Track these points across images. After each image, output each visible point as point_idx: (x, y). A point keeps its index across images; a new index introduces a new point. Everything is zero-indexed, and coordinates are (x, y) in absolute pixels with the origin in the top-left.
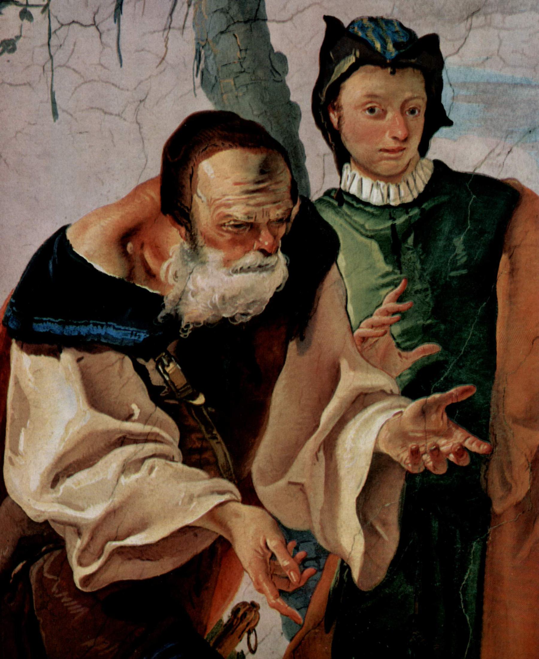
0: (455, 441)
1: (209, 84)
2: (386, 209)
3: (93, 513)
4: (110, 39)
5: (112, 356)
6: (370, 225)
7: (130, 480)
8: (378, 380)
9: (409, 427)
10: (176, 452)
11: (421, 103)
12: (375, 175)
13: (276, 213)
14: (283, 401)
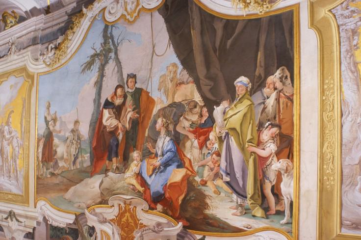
1: (118, 82)
2: (132, 92)
3: (108, 124)
8: (131, 110)
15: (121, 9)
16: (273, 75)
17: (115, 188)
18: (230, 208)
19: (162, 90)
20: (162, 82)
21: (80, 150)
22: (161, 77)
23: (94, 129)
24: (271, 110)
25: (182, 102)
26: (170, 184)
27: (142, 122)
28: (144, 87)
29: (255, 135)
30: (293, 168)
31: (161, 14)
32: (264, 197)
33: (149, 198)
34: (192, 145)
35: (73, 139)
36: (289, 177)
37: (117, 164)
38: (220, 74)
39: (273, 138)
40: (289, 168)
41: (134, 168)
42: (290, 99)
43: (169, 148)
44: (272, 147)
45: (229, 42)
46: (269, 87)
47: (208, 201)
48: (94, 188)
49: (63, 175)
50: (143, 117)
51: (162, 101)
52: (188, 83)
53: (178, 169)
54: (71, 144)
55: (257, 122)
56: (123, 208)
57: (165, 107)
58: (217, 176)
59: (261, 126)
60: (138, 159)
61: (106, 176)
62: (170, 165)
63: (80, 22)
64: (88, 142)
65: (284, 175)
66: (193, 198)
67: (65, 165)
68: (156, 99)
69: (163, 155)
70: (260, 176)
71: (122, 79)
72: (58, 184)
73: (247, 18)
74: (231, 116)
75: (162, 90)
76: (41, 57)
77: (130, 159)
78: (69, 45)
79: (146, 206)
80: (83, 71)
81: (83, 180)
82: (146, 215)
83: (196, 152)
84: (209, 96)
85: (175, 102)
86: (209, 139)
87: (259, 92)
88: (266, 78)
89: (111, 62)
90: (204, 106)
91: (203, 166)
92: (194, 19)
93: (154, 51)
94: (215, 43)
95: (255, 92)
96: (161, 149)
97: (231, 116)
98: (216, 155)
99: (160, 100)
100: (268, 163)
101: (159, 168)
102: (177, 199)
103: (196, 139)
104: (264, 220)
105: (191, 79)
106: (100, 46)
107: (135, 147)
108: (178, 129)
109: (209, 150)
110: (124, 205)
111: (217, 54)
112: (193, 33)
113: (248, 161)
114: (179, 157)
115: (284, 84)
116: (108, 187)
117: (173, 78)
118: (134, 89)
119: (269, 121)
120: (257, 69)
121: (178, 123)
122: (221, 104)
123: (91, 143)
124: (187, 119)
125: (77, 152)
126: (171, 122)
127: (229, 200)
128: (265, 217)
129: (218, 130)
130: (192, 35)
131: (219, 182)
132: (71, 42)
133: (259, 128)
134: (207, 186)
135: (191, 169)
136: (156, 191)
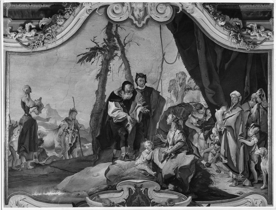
0: (147, 110)
2: (141, 90)
3: (115, 116)
4: (118, 75)
5: (117, 102)
6: (140, 91)
7: (118, 113)
8: (140, 105)
9: (143, 109)
10: (123, 111)
11: (144, 81)
12: (140, 87)
13: (132, 90)
14: (132, 107)
15: (127, 12)
16: (255, 93)
17: (124, 174)
18: (228, 182)
19: (172, 92)
20: (172, 85)
21: (79, 140)
22: (171, 81)
23: (97, 120)
24: (254, 116)
25: (190, 104)
26: (180, 168)
27: (153, 117)
28: (154, 87)
29: (244, 130)
30: (268, 153)
31: (170, 30)
32: (250, 172)
33: (160, 180)
34: (199, 137)
35: (69, 128)
36: (265, 159)
37: (126, 152)
38: (220, 87)
39: (255, 134)
40: (265, 153)
41: (145, 155)
42: (266, 109)
43: (179, 139)
44: (255, 140)
45: (227, 65)
46: (253, 101)
47: (212, 178)
48: (98, 175)
49: (54, 165)
50: (153, 112)
51: (173, 100)
52: (195, 90)
53: (187, 156)
54: (64, 133)
55: (246, 123)
56: (134, 191)
57: (175, 106)
58: (218, 159)
59: (248, 125)
60: (150, 148)
61: (114, 164)
62: (181, 152)
63: (74, 10)
64: (89, 132)
65: (262, 158)
66: (201, 177)
67: (57, 155)
68: (166, 99)
69: (174, 144)
70: (248, 158)
71: (131, 77)
72: (46, 175)
73: (238, 51)
74: (228, 118)
75: (172, 92)
76: (13, 35)
77: (141, 148)
78: (58, 31)
79: (157, 186)
80: (80, 61)
81: (83, 169)
82: (158, 195)
83: (202, 142)
84: (212, 101)
85: (184, 103)
86: (212, 133)
87: (247, 103)
88: (251, 94)
89: (116, 58)
90: (208, 108)
91: (208, 152)
92: (199, 41)
93: (163, 58)
94: (216, 63)
95: (244, 103)
96: (171, 140)
97: (228, 118)
98: (217, 144)
99: (170, 99)
100: (253, 150)
101: (171, 155)
102: (187, 179)
103: (202, 132)
104: (250, 187)
105: (197, 87)
106: (103, 42)
107: (146, 138)
108: (187, 124)
109: (212, 141)
110: (135, 189)
111: (218, 71)
112: (199, 52)
113: (240, 149)
114: (188, 146)
115: (262, 100)
116: (116, 174)
117: (182, 83)
118: (145, 87)
119: (253, 122)
120: (245, 88)
121: (187, 119)
122: (221, 109)
123: (93, 133)
124: (194, 117)
125: (74, 142)
126: (181, 119)
127: (227, 177)
128: (251, 185)
129: (218, 126)
130: (198, 53)
131: (220, 164)
132: (63, 28)
133: (247, 127)
134: (211, 167)
135: (198, 155)
136: (167, 174)
